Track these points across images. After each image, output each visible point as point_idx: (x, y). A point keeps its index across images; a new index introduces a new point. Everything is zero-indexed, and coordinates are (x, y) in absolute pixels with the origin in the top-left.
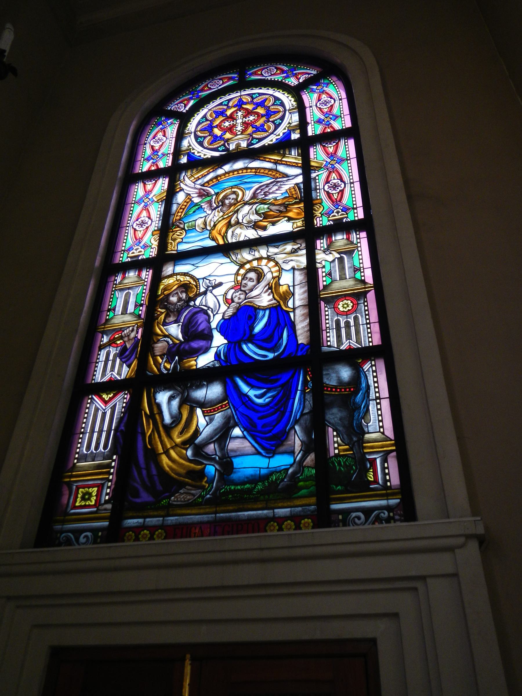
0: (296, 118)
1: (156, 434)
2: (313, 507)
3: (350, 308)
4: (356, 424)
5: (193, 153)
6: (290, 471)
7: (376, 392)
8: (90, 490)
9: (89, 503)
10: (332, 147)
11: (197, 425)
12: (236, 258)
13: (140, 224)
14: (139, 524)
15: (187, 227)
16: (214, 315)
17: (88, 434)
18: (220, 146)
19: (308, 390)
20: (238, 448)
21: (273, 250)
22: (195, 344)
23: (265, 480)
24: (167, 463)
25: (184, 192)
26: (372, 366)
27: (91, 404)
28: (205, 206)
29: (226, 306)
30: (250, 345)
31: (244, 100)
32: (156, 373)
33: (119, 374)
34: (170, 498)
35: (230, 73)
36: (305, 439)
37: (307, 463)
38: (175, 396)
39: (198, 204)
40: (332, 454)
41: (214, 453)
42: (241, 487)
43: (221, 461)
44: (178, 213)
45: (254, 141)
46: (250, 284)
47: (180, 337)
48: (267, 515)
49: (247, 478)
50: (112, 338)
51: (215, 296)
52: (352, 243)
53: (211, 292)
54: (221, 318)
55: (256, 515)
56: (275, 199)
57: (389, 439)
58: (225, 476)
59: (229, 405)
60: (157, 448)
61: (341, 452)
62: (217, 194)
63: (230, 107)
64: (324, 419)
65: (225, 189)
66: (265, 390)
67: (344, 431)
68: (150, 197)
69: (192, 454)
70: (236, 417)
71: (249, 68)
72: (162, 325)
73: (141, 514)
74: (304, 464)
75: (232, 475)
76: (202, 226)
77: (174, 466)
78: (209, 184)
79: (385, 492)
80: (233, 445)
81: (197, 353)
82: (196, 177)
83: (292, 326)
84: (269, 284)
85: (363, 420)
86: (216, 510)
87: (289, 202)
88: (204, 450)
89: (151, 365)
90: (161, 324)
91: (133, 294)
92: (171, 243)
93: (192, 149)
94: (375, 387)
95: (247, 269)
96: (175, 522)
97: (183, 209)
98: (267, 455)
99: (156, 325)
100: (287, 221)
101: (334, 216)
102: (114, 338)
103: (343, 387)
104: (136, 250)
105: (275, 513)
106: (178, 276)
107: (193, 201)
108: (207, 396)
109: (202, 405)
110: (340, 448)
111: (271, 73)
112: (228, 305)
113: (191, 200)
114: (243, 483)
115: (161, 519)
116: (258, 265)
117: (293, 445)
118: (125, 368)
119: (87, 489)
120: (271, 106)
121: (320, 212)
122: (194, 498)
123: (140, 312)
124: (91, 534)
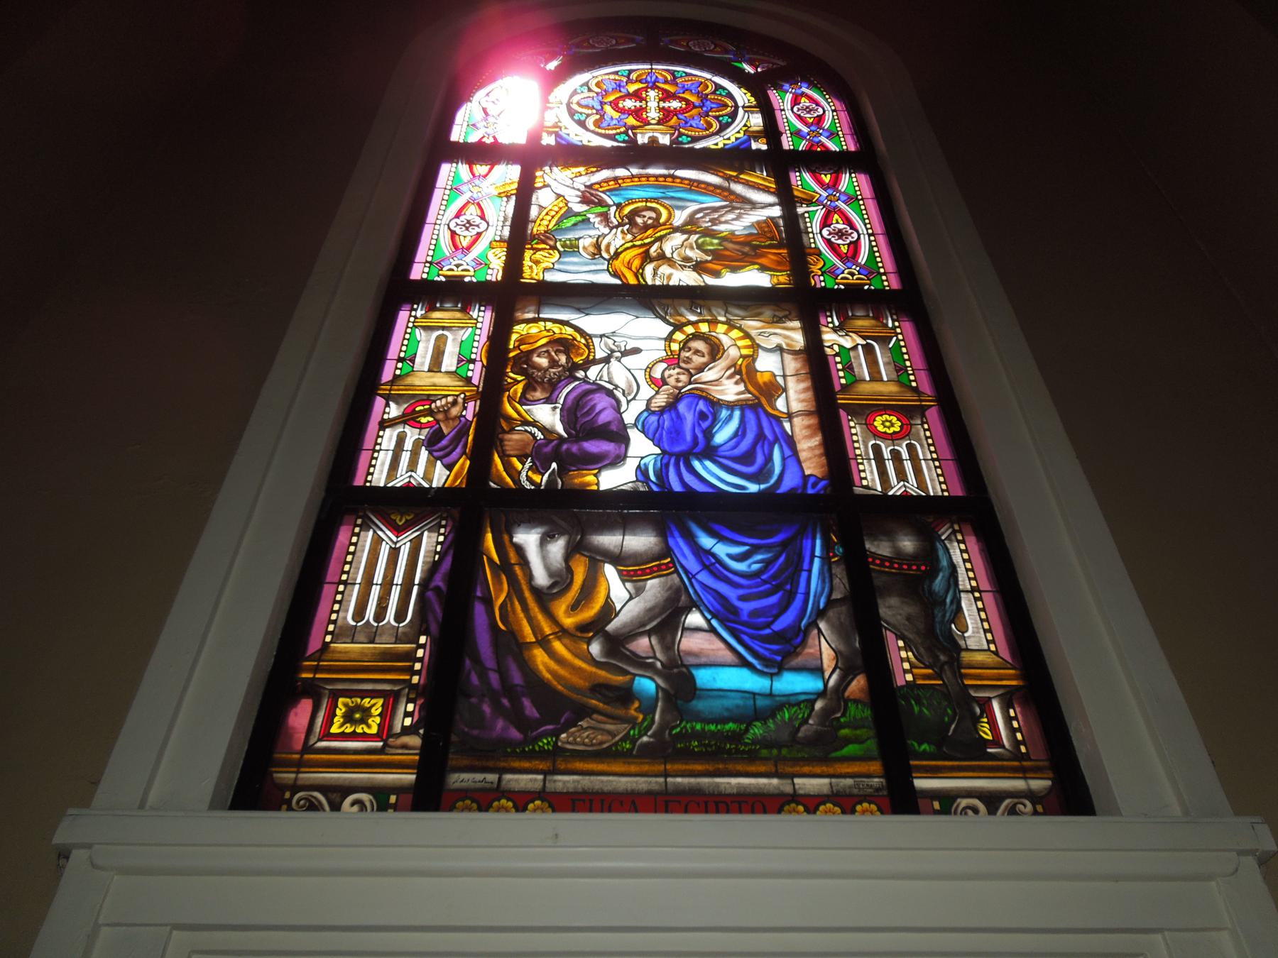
0: (757, 121)
1: (517, 603)
2: (876, 780)
3: (897, 429)
4: (941, 630)
5: (568, 135)
6: (819, 705)
8: (366, 702)
9: (363, 728)
10: (829, 176)
11: (608, 596)
13: (464, 225)
15: (563, 247)
16: (628, 402)
17: (357, 587)
19: (836, 559)
20: (702, 649)
22: (593, 446)
24: (546, 663)
26: (954, 532)
29: (653, 388)
30: (708, 463)
33: (428, 476)
34: (558, 737)
36: (842, 647)
37: (852, 693)
40: (900, 682)
41: (651, 655)
42: (716, 726)
46: (698, 360)
47: (560, 428)
48: (779, 788)
49: (727, 709)
51: (629, 370)
53: (619, 361)
54: (644, 407)
56: (732, 233)
57: (1009, 666)
59: (675, 566)
60: (521, 631)
61: (919, 679)
62: (619, 206)
64: (878, 618)
65: (634, 200)
69: (601, 651)
72: (518, 403)
74: (847, 694)
75: (694, 702)
76: (592, 249)
77: (562, 672)
78: (601, 187)
80: (689, 643)
81: (597, 462)
83: (790, 442)
84: (734, 365)
85: (953, 626)
88: (627, 646)
89: (498, 470)
90: (517, 400)
91: (454, 340)
92: (531, 267)
93: (563, 129)
94: (967, 570)
95: (691, 334)
96: (572, 786)
98: (765, 670)
100: (757, 269)
103: (905, 562)
104: (458, 266)
105: (797, 787)
108: (624, 543)
109: (617, 559)
110: (915, 671)
111: (705, 48)
112: (657, 389)
113: (567, 205)
114: (724, 721)
115: (540, 777)
118: (441, 470)
120: (711, 94)
121: (819, 267)
122: (613, 739)
123: (470, 374)
124: (371, 797)
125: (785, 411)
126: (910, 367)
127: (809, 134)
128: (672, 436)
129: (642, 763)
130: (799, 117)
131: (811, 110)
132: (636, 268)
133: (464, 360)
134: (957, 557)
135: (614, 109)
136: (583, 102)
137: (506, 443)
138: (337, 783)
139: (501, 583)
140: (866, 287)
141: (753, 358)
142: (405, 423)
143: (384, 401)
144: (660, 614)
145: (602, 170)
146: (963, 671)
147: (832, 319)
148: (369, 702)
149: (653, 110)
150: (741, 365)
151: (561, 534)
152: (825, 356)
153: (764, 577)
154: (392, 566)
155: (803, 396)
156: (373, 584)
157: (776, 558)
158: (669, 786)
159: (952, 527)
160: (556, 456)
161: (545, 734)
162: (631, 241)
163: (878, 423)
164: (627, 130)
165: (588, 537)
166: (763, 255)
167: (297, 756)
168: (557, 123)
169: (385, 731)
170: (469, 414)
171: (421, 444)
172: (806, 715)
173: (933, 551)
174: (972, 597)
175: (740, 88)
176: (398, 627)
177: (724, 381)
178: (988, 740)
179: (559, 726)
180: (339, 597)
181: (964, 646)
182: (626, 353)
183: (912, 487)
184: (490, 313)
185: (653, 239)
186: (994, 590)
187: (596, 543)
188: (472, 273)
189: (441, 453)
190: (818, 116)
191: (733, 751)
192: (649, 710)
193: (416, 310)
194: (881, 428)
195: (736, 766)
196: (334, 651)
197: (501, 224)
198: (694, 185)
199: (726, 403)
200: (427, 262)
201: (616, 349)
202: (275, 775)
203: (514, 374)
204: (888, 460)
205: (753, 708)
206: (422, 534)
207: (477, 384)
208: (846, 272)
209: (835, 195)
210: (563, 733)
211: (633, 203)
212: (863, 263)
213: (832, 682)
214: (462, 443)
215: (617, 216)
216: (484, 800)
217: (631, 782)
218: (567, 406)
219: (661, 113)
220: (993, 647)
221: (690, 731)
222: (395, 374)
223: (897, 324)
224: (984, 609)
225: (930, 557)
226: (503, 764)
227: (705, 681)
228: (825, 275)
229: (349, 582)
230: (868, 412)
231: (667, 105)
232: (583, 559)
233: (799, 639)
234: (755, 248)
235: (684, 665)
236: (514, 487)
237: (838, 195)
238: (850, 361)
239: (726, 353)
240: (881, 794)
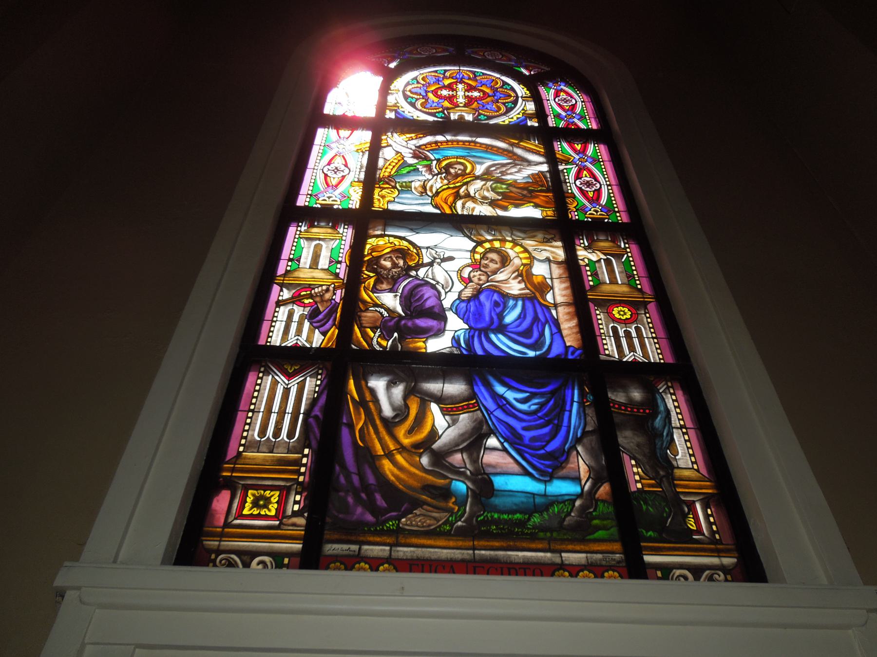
0: (531, 107)
1: (371, 428)
2: (618, 555)
4: (660, 454)
5: (404, 112)
6: (578, 503)
9: (265, 511)
10: (580, 145)
11: (433, 425)
13: (333, 170)
15: (400, 187)
16: (446, 293)
17: (261, 414)
19: (588, 403)
20: (498, 463)
24: (391, 470)
26: (668, 388)
30: (501, 336)
34: (399, 520)
36: (593, 464)
37: (600, 495)
40: (633, 489)
41: (463, 466)
42: (508, 516)
43: (474, 477)
46: (493, 266)
47: (399, 310)
49: (516, 504)
51: (446, 271)
53: (440, 265)
54: (457, 297)
55: (535, 559)
56: (515, 181)
57: (706, 479)
58: (483, 499)
59: (478, 405)
60: (374, 447)
61: (646, 487)
62: (439, 161)
66: (528, 394)
69: (429, 462)
72: (371, 291)
74: (597, 496)
75: (493, 499)
76: (420, 189)
77: (402, 476)
78: (426, 148)
80: (489, 458)
83: (556, 323)
84: (518, 270)
85: (668, 451)
88: (447, 459)
90: (370, 290)
93: (400, 108)
94: (677, 413)
95: (488, 249)
96: (410, 555)
98: (541, 478)
100: (533, 206)
104: (329, 198)
105: (564, 559)
106: (391, 238)
108: (444, 389)
109: (439, 399)
110: (643, 481)
112: (465, 285)
113: (403, 159)
114: (514, 512)
115: (388, 548)
117: (578, 469)
120: (500, 88)
121: (574, 206)
122: (437, 523)
123: (338, 271)
124: (271, 559)
125: (552, 302)
126: (637, 275)
127: (566, 117)
128: (476, 317)
129: (458, 540)
130: (559, 105)
131: (567, 101)
132: (451, 203)
133: (333, 262)
134: (670, 405)
135: (435, 96)
136: (414, 90)
137: (363, 318)
138: (247, 549)
139: (360, 414)
140: (606, 220)
141: (530, 266)
142: (294, 303)
143: (279, 288)
144: (470, 438)
145: (427, 136)
146: (675, 482)
147: (583, 241)
148: (269, 494)
149: (461, 97)
150: (522, 270)
151: (401, 381)
152: (579, 266)
153: (539, 414)
154: (285, 400)
155: (564, 293)
156: (272, 412)
157: (548, 401)
158: (476, 557)
159: (666, 384)
160: (397, 328)
161: (391, 519)
162: (447, 185)
163: (615, 312)
164: (444, 110)
165: (419, 384)
166: (537, 197)
167: (219, 530)
168: (396, 104)
169: (281, 514)
170: (338, 298)
171: (304, 318)
172: (569, 510)
173: (654, 400)
174: (681, 433)
175: (519, 84)
176: (290, 442)
177: (511, 281)
178: (694, 530)
179: (400, 513)
180: (248, 421)
181: (676, 465)
182: (444, 260)
183: (640, 358)
184: (352, 230)
185: (461, 183)
186: (696, 427)
187: (425, 388)
188: (339, 203)
189: (318, 324)
190: (572, 105)
191: (520, 533)
192: (462, 504)
193: (301, 226)
194: (617, 316)
195: (522, 543)
196: (245, 458)
197: (359, 170)
198: (489, 149)
199: (513, 296)
200: (308, 194)
201: (437, 257)
202: (205, 542)
203: (368, 271)
204: (622, 337)
205: (533, 504)
206: (306, 379)
207: (343, 278)
208: (592, 209)
209: (584, 158)
210: (403, 518)
211: (448, 159)
212: (604, 204)
213: (586, 488)
215: (437, 167)
216: (349, 563)
217: (451, 553)
218: (404, 295)
219: (467, 100)
220: (695, 467)
221: (490, 519)
222: (286, 270)
223: (627, 246)
224: (689, 441)
225: (652, 404)
226: (361, 538)
227: (500, 485)
228: (578, 211)
229: (255, 410)
230: (609, 305)
231: (470, 94)
232: (416, 399)
233: (564, 458)
234: (531, 192)
235: (485, 473)
236: (368, 349)
237: (586, 158)
238: (596, 270)
239: (512, 262)
240: (621, 565)
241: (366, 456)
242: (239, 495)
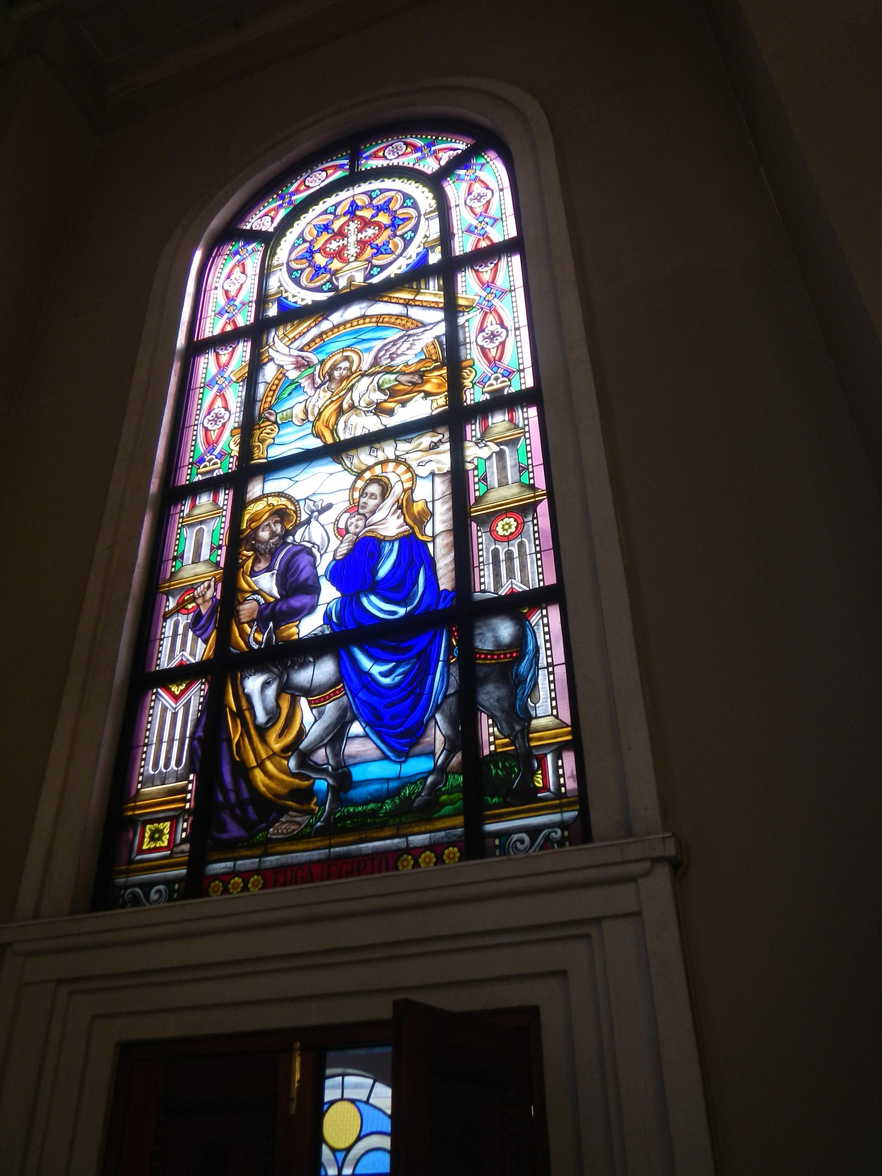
2: (460, 830)
3: (513, 530)
5: (286, 298)
6: (430, 780)
7: (547, 657)
8: (161, 826)
11: (302, 723)
12: (352, 463)
14: (228, 870)
16: (321, 555)
17: (154, 746)
18: (325, 284)
19: (454, 660)
20: (358, 751)
21: (403, 447)
23: (395, 796)
25: (274, 362)
26: (542, 617)
27: (157, 701)
28: (305, 383)
30: (373, 598)
31: (359, 203)
32: (244, 649)
35: (337, 159)
38: (270, 681)
39: (295, 381)
40: (486, 752)
41: (326, 762)
42: (363, 808)
43: (335, 772)
44: (266, 398)
45: (375, 271)
46: (372, 503)
49: (371, 794)
50: (180, 601)
51: (323, 526)
52: (516, 426)
53: (317, 520)
59: (345, 690)
60: (248, 759)
61: (499, 748)
62: (322, 362)
63: (338, 215)
67: (503, 717)
68: (226, 375)
69: (296, 765)
70: (354, 707)
71: (365, 146)
72: (249, 576)
73: (229, 856)
74: (449, 769)
76: (302, 416)
77: (272, 785)
78: (310, 348)
79: (557, 802)
82: (291, 336)
83: (431, 564)
84: (398, 501)
86: (330, 843)
87: (426, 367)
89: (236, 638)
91: (208, 531)
92: (259, 447)
93: (284, 292)
94: (546, 649)
95: (367, 480)
97: (274, 391)
98: (397, 760)
99: (242, 579)
100: (423, 398)
101: (492, 385)
102: (184, 600)
103: (502, 652)
104: (209, 461)
105: (409, 842)
106: (269, 498)
107: (287, 377)
109: (307, 692)
110: (497, 742)
111: (398, 153)
112: (341, 539)
113: (284, 374)
114: (367, 802)
115: (257, 860)
116: (382, 473)
118: (201, 646)
119: (156, 825)
121: (471, 379)
123: (218, 559)
161: (261, 831)
182: (322, 511)
187: (296, 682)
198: (380, 321)
203: (248, 551)
214: (213, 621)
218: (281, 570)
239: (392, 491)
241: (242, 771)
242: (139, 832)
